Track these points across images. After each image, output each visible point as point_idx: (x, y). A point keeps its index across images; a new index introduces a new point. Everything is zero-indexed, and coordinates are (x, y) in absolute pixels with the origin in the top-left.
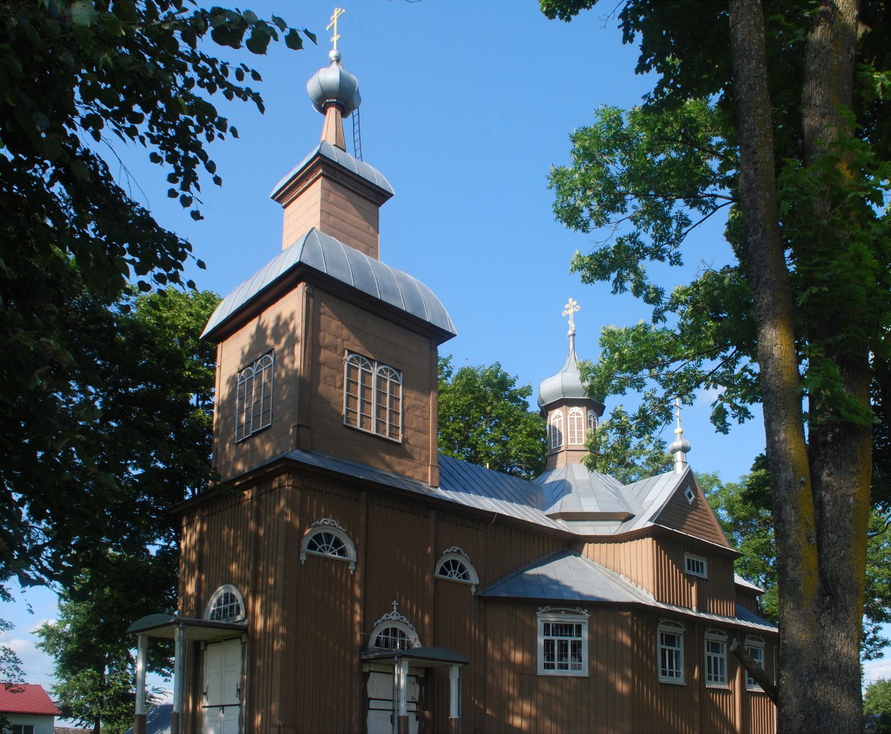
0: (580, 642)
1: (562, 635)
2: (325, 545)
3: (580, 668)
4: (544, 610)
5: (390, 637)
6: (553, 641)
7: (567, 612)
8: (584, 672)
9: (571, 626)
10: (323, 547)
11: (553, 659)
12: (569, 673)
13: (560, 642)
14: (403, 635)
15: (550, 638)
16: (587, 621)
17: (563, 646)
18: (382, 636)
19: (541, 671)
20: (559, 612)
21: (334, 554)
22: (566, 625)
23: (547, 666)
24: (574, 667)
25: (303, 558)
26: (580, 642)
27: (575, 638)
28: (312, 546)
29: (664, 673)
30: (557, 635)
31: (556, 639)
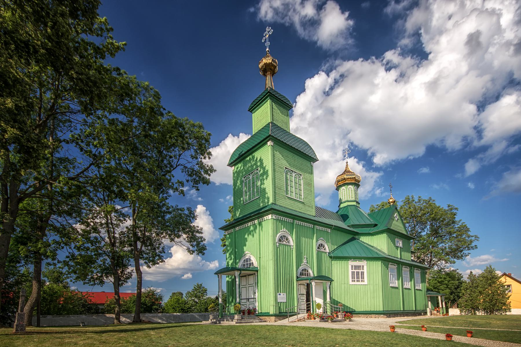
8: (366, 282)
9: (360, 266)
15: (353, 271)
23: (352, 281)
31: (356, 271)
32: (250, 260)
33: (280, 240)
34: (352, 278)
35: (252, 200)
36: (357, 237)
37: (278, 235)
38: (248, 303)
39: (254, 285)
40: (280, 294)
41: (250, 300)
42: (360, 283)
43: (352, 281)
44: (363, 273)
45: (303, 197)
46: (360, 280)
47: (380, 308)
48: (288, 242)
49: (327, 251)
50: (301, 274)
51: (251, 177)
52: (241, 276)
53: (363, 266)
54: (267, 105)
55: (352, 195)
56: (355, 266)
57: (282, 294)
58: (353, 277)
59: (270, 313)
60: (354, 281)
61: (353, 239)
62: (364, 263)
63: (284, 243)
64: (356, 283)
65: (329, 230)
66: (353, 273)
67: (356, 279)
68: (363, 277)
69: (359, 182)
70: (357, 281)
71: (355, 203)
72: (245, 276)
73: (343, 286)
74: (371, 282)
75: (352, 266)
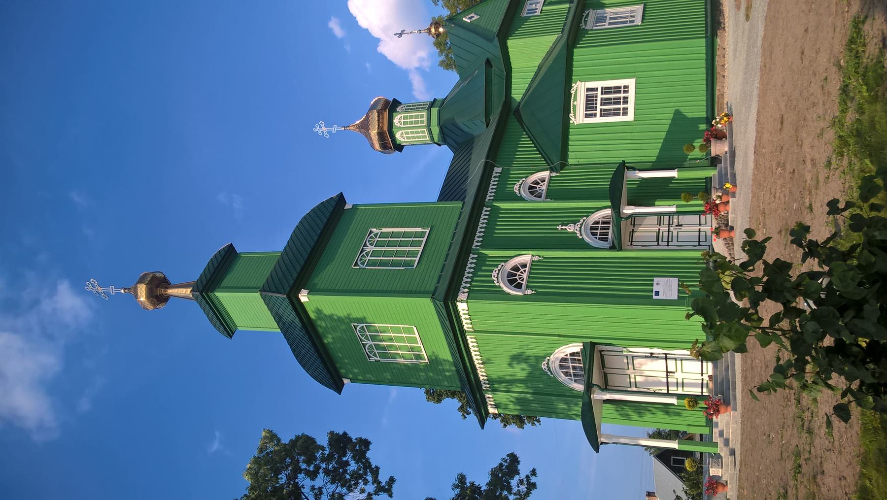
0: (602, 88)
3: (625, 87)
4: (573, 119)
5: (599, 231)
7: (575, 100)
8: (631, 83)
9: (587, 96)
11: (619, 109)
12: (631, 95)
13: (601, 105)
14: (597, 223)
15: (598, 112)
17: (605, 102)
18: (598, 236)
19: (630, 117)
20: (575, 106)
22: (587, 101)
23: (625, 114)
26: (602, 88)
31: (599, 107)
32: (564, 360)
33: (519, 286)
34: (618, 114)
36: (514, 106)
37: (506, 289)
40: (657, 293)
42: (631, 95)
43: (625, 114)
44: (606, 91)
46: (622, 95)
48: (524, 266)
50: (606, 240)
52: (606, 388)
53: (588, 90)
54: (225, 298)
55: (417, 117)
56: (587, 109)
57: (656, 288)
58: (616, 113)
60: (625, 109)
61: (517, 112)
62: (580, 89)
63: (525, 276)
64: (631, 106)
65: (497, 170)
66: (604, 113)
67: (621, 106)
68: (617, 89)
69: (387, 102)
70: (626, 102)
71: (435, 111)
72: (605, 375)
75: (587, 116)
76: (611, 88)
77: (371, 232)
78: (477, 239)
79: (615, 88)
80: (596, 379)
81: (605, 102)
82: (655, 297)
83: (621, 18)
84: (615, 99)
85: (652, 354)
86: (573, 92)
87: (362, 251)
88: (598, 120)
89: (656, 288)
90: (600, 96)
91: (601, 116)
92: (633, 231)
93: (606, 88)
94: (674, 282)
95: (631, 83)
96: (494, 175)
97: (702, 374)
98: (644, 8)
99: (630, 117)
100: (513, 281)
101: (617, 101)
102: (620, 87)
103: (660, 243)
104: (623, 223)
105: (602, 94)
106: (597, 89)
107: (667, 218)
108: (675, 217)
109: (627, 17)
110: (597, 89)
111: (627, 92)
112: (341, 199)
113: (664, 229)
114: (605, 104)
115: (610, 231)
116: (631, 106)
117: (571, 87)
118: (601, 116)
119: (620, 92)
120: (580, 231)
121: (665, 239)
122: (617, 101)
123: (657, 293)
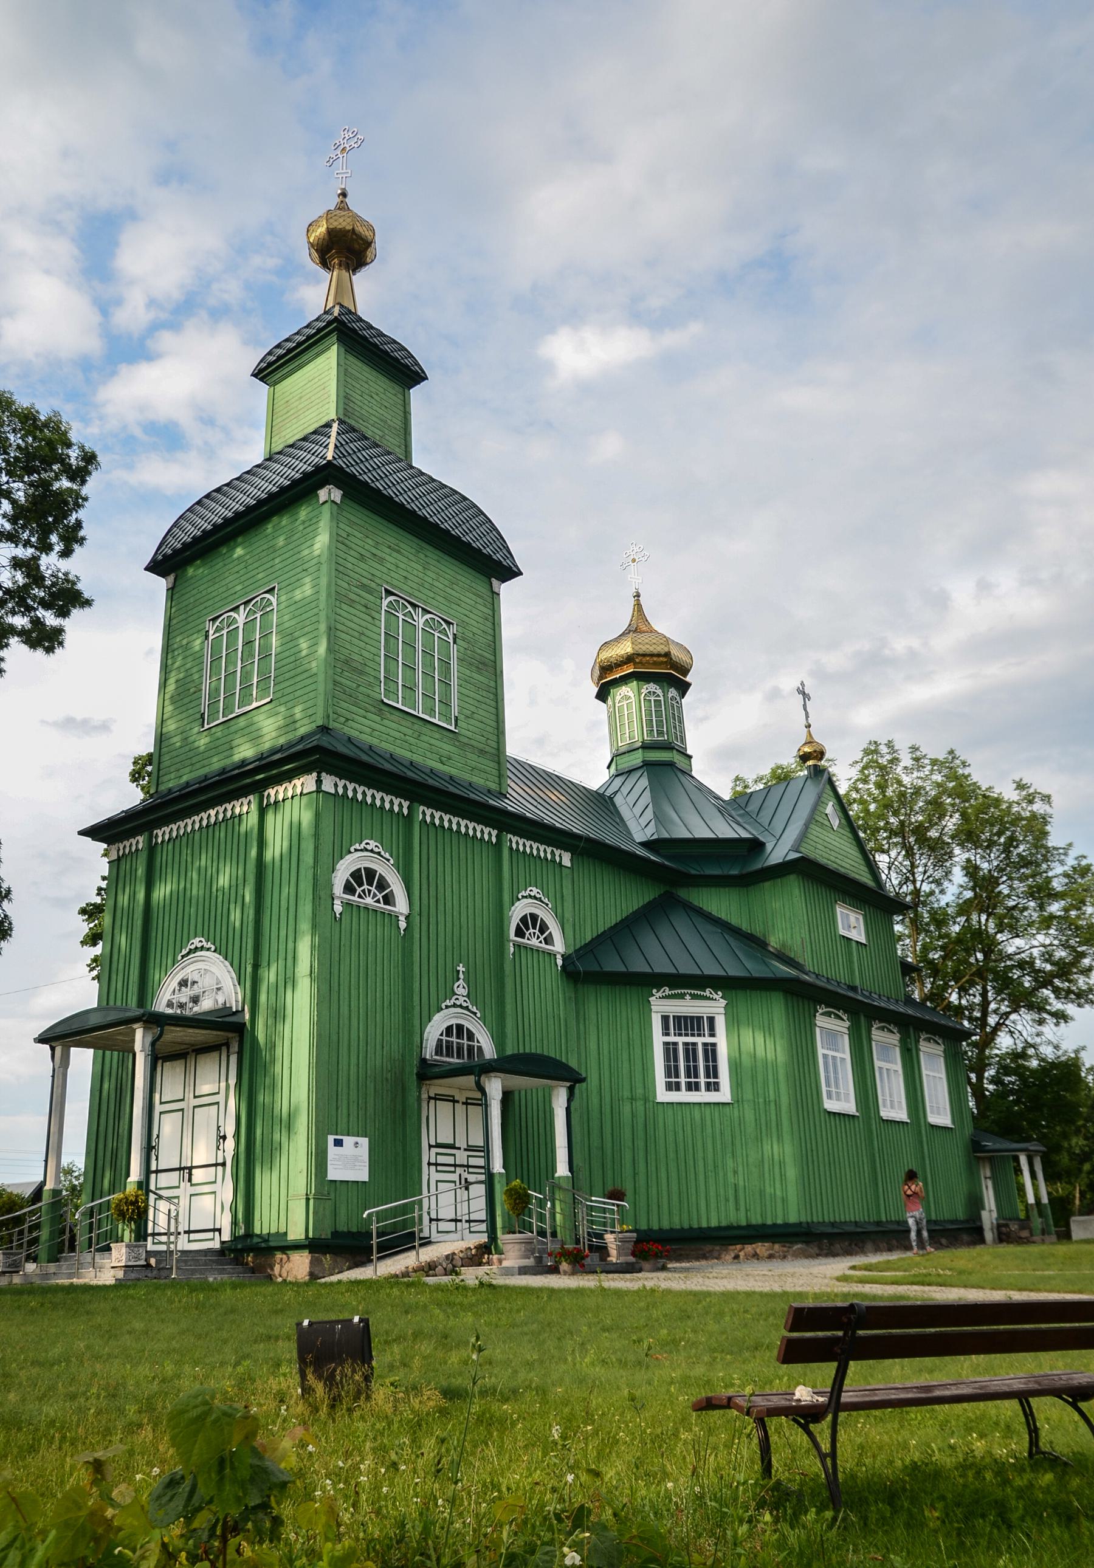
0: (714, 1045)
1: (686, 1035)
2: (366, 887)
3: (717, 1084)
4: (660, 994)
5: (454, 1039)
6: (675, 1044)
7: (694, 997)
8: (724, 1094)
9: (699, 1019)
10: (363, 891)
11: (677, 1076)
12: (703, 1096)
13: (686, 1044)
14: (471, 1036)
15: (671, 1039)
16: (722, 1010)
19: (663, 1095)
20: (682, 996)
21: (378, 901)
22: (692, 1018)
23: (669, 1087)
24: (709, 1087)
25: (338, 908)
26: (714, 1045)
27: (708, 1040)
28: (349, 889)
29: (830, 1097)
30: (680, 1035)
31: (680, 1040)
34: (668, 1074)
35: (238, 711)
36: (683, 893)
38: (185, 1189)
39: (220, 1098)
41: (198, 1175)
42: (703, 1096)
43: (669, 1087)
44: (711, 1051)
45: (455, 711)
46: (702, 1080)
47: (792, 1211)
49: (559, 946)
50: (439, 1050)
51: (241, 617)
52: (158, 1058)
53: (711, 1020)
56: (678, 1019)
58: (671, 1071)
59: (291, 1237)
60: (678, 1087)
62: (714, 1006)
64: (684, 1096)
66: (670, 1050)
67: (683, 1080)
68: (712, 1071)
70: (690, 1087)
73: (627, 1109)
74: (748, 1095)
75: (665, 1019)
76: (715, 1060)
77: (448, 623)
78: (437, 815)
79: (715, 1068)
80: (174, 1034)
81: (690, 1051)
82: (331, 1139)
83: (836, 1079)
84: (696, 1068)
85: (224, 1138)
86: (707, 992)
87: (414, 606)
88: (658, 1040)
89: (348, 1141)
90: (700, 1041)
91: (666, 1044)
92: (454, 1101)
93: (714, 1052)
94: (362, 1174)
95: (724, 1094)
96: (557, 852)
97: (188, 1232)
98: (853, 1116)
99: (663, 1095)
100: (362, 878)
101: (692, 1072)
102: (716, 1076)
103: (434, 1150)
104: (470, 1080)
105: (705, 1045)
106: (712, 1035)
107: (481, 1162)
108: (483, 1177)
109: (837, 1086)
110: (712, 1035)
111: (708, 1089)
112: (509, 572)
113: (461, 1157)
114: (687, 1051)
115: (455, 1060)
116: (684, 1096)
117: (716, 989)
118: (666, 1044)
119: (708, 1076)
120: (455, 1005)
121: (441, 1159)
122: (692, 1072)
123: (338, 1143)
